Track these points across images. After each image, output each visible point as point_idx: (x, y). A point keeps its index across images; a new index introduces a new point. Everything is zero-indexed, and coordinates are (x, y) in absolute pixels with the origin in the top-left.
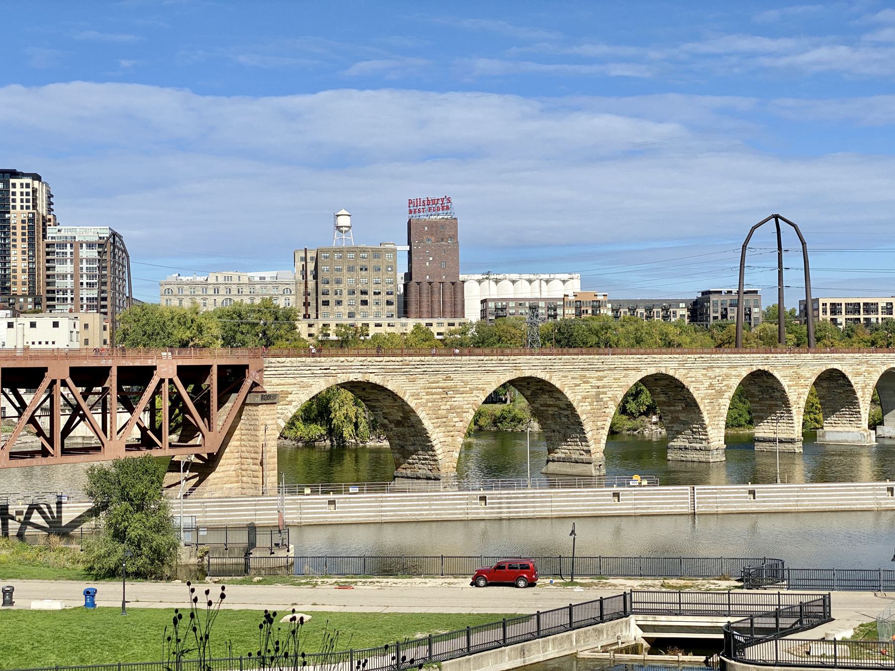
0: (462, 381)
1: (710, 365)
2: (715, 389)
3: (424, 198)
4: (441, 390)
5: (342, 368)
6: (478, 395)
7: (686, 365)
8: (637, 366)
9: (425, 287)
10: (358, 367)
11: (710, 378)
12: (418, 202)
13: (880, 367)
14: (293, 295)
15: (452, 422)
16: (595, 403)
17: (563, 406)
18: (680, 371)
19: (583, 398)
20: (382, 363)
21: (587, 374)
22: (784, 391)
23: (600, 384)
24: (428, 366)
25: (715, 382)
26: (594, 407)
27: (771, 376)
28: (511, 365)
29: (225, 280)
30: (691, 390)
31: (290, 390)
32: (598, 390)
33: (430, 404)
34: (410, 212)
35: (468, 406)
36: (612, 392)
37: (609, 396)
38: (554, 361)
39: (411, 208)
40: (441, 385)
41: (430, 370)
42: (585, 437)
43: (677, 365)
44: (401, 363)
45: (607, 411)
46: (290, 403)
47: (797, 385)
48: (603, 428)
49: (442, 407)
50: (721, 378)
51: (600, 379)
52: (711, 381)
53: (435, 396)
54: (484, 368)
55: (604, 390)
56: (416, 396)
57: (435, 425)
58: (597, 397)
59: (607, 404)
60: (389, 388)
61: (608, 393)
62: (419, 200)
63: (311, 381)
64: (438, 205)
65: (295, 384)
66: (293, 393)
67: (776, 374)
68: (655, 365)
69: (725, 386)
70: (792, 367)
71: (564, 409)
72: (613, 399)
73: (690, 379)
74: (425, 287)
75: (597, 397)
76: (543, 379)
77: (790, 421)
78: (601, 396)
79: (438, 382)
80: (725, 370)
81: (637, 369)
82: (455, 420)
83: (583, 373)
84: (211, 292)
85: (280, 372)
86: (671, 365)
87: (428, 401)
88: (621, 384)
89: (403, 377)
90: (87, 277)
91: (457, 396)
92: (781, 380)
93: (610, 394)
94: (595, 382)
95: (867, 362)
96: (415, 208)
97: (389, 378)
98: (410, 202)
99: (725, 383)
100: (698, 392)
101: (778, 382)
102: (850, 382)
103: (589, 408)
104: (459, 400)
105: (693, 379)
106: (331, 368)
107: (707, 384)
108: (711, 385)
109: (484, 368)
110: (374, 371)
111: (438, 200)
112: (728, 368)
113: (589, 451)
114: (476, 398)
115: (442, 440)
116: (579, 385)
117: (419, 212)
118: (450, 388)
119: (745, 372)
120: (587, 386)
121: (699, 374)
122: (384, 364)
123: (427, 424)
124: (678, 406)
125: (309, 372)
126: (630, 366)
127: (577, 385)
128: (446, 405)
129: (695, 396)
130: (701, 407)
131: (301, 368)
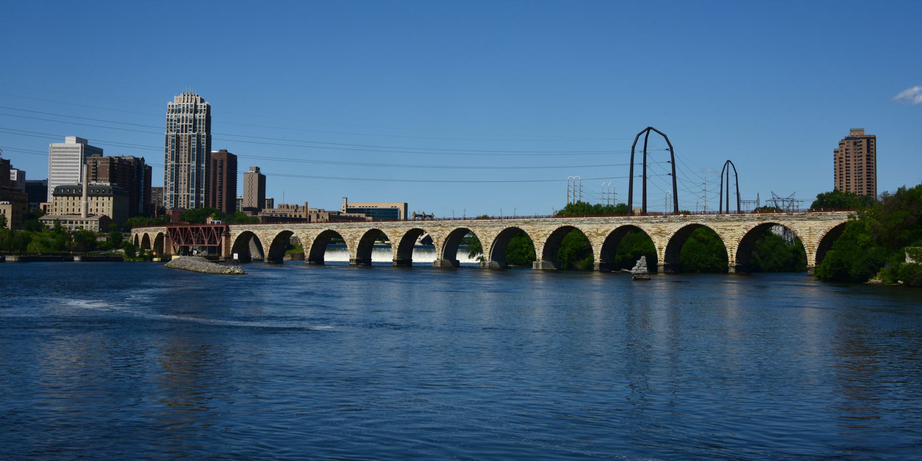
23: (308, 233)
25: (352, 233)
27: (381, 232)
56: (259, 235)
67: (384, 231)
70: (392, 227)
72: (313, 238)
92: (386, 233)
93: (311, 237)
95: (440, 225)
104: (269, 237)
107: (349, 235)
108: (351, 235)
118: (267, 233)
119: (367, 230)
121: (346, 230)
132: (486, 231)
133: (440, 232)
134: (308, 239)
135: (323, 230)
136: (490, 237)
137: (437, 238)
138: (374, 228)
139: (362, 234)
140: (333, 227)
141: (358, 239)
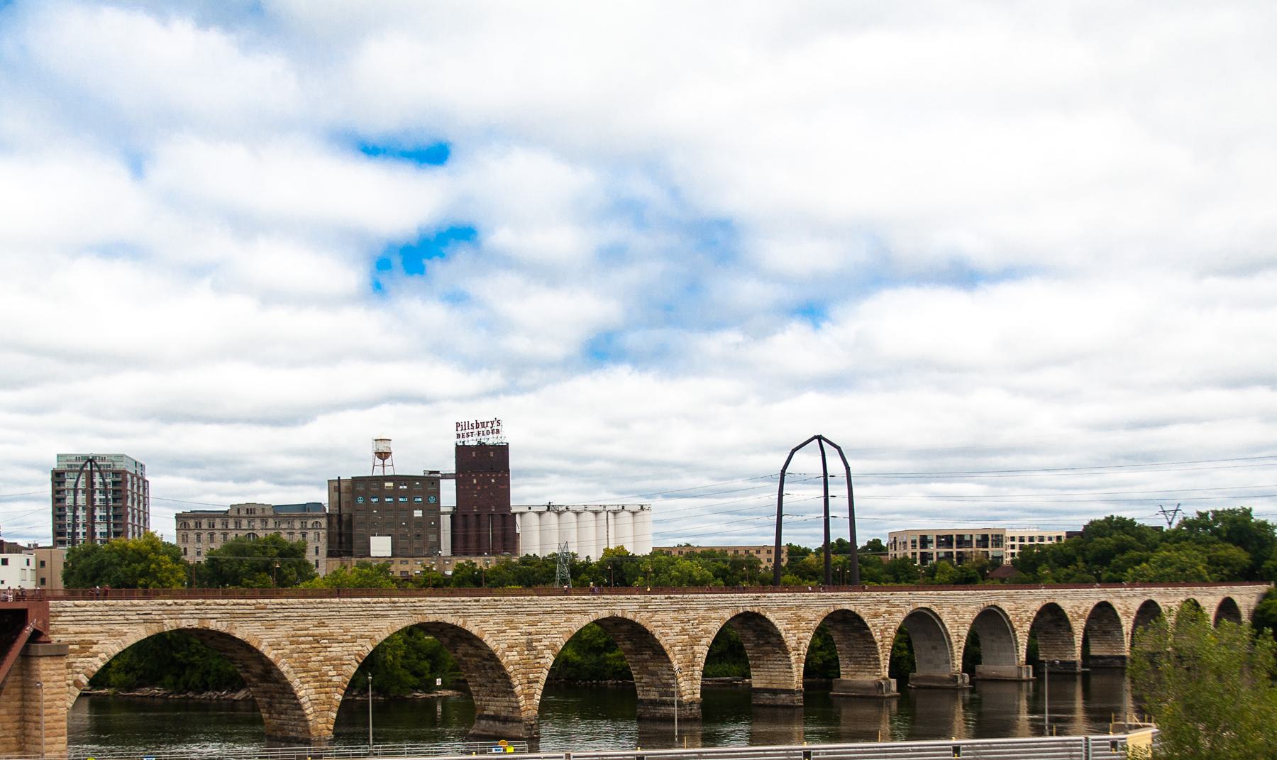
0: (340, 627)
1: (682, 606)
2: (688, 634)
3: (472, 421)
4: (311, 638)
5: (168, 612)
6: (364, 644)
7: (649, 607)
8: (583, 608)
9: (472, 519)
10: (192, 612)
11: (682, 622)
12: (467, 425)
13: (904, 607)
14: (323, 529)
15: (327, 676)
16: (526, 653)
17: (486, 656)
18: (642, 614)
19: (509, 647)
20: (227, 607)
21: (515, 618)
22: (780, 635)
23: (532, 629)
24: (292, 610)
26: (525, 657)
27: (764, 618)
28: (409, 608)
29: (248, 513)
30: (656, 636)
31: (95, 640)
32: (530, 637)
33: (295, 655)
34: (458, 436)
35: (348, 657)
36: (549, 640)
37: (546, 643)
38: (469, 603)
39: (460, 432)
40: (311, 632)
41: (296, 614)
42: (513, 692)
43: (638, 607)
44: (253, 607)
45: (542, 661)
46: (95, 655)
47: (797, 628)
48: (537, 682)
49: (313, 659)
50: (697, 621)
51: (533, 624)
52: (682, 624)
53: (303, 646)
54: (371, 613)
55: (537, 637)
56: (275, 645)
57: (302, 680)
58: (530, 646)
59: (543, 653)
60: (238, 636)
61: (543, 640)
62: (467, 423)
63: (125, 629)
64: (488, 429)
65: (102, 632)
66: (100, 642)
67: (770, 616)
68: (608, 607)
69: (702, 630)
70: (790, 608)
71: (487, 660)
72: (552, 647)
73: (655, 623)
74: (472, 519)
75: (530, 646)
76: (455, 624)
77: (789, 670)
78: (534, 644)
79: (307, 629)
80: (702, 613)
81: (584, 613)
82: (331, 673)
83: (509, 618)
84: (231, 526)
85: (79, 618)
86: (630, 607)
87: (292, 652)
88: (562, 630)
89: (258, 624)
90: (101, 509)
91: (334, 645)
92: (776, 623)
94: (525, 628)
95: (887, 602)
96: (463, 432)
97: (236, 624)
98: (458, 425)
99: (702, 627)
100: (666, 638)
101: (772, 625)
102: (865, 624)
103: (517, 658)
104: (336, 649)
105: (660, 623)
106: (154, 613)
107: (677, 629)
108: (683, 631)
109: (371, 613)
110: (215, 616)
111: (487, 422)
112: (705, 610)
113: (519, 707)
114: (360, 648)
115: (312, 697)
116: (504, 631)
117: (468, 436)
118: (323, 636)
120: (514, 633)
121: (668, 618)
122: (230, 607)
123: (290, 677)
124: (646, 654)
125: (122, 618)
126: (573, 609)
127: (500, 631)
128: (318, 656)
129: (661, 642)
130: (671, 655)
131: (109, 613)
132: (957, 613)
133: (886, 615)
134: (534, 648)
135: (593, 617)
136: (963, 624)
137: (882, 631)
138: (748, 609)
139: (715, 627)
140: (627, 606)
141: (704, 641)
